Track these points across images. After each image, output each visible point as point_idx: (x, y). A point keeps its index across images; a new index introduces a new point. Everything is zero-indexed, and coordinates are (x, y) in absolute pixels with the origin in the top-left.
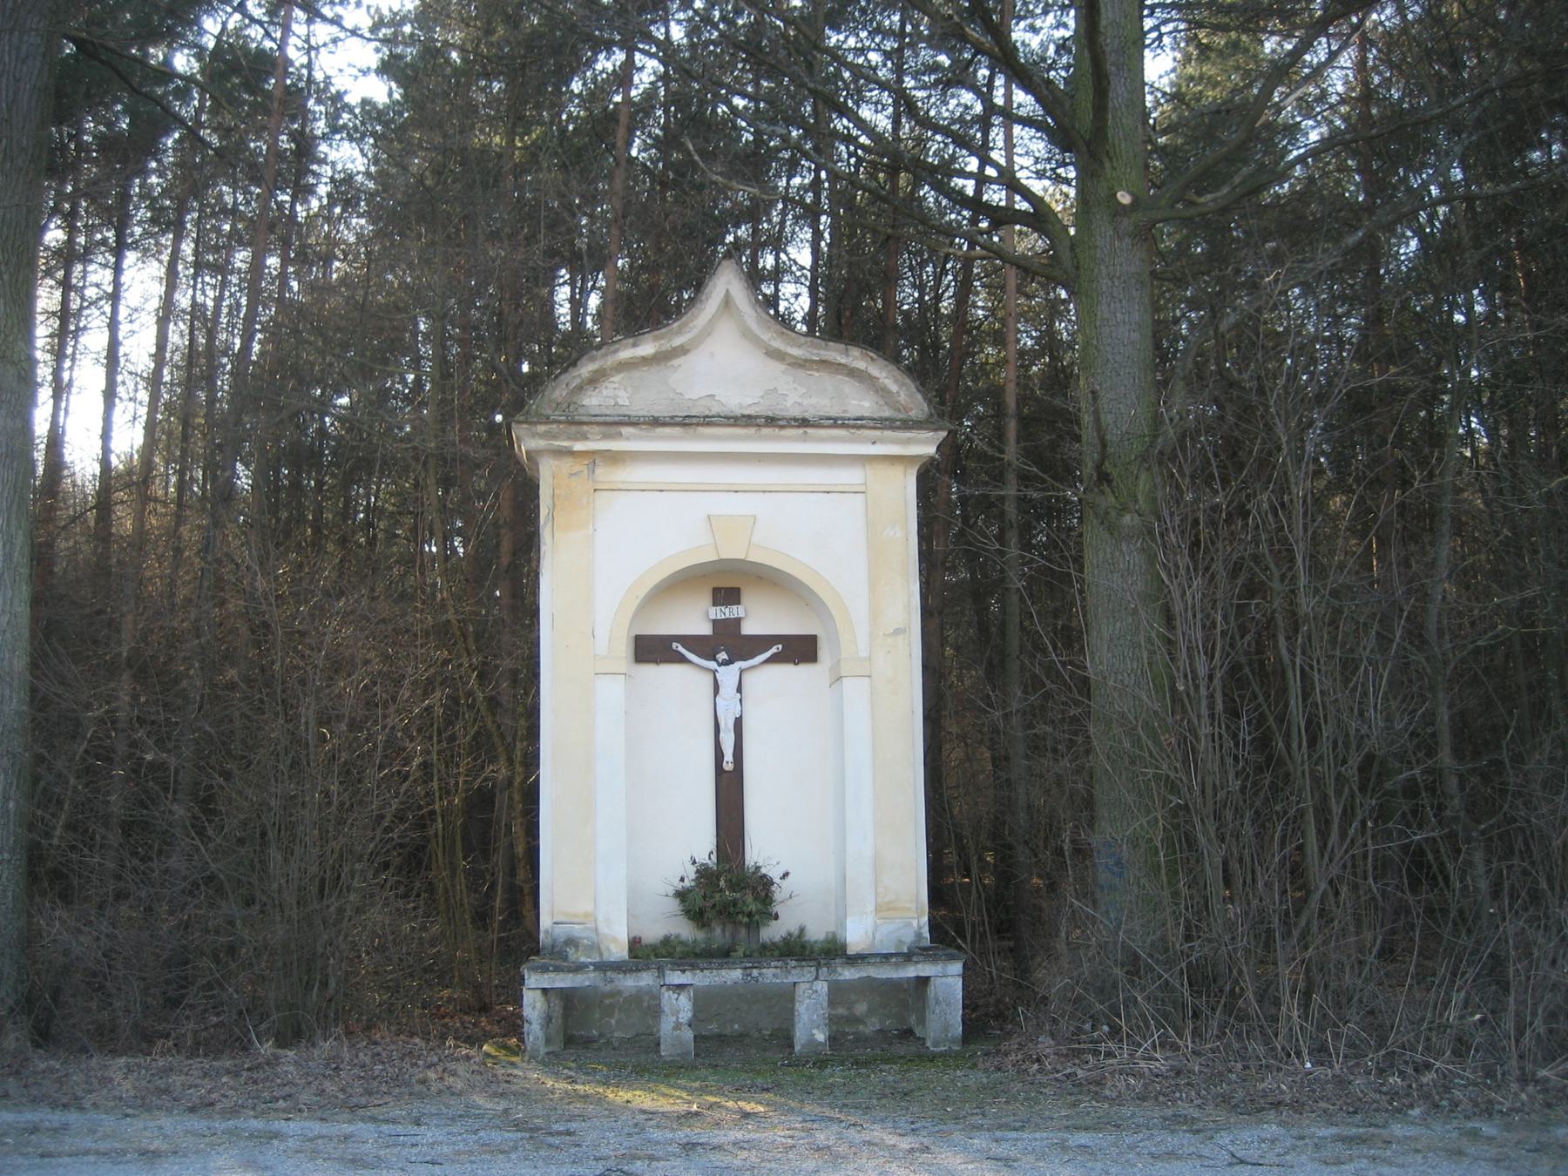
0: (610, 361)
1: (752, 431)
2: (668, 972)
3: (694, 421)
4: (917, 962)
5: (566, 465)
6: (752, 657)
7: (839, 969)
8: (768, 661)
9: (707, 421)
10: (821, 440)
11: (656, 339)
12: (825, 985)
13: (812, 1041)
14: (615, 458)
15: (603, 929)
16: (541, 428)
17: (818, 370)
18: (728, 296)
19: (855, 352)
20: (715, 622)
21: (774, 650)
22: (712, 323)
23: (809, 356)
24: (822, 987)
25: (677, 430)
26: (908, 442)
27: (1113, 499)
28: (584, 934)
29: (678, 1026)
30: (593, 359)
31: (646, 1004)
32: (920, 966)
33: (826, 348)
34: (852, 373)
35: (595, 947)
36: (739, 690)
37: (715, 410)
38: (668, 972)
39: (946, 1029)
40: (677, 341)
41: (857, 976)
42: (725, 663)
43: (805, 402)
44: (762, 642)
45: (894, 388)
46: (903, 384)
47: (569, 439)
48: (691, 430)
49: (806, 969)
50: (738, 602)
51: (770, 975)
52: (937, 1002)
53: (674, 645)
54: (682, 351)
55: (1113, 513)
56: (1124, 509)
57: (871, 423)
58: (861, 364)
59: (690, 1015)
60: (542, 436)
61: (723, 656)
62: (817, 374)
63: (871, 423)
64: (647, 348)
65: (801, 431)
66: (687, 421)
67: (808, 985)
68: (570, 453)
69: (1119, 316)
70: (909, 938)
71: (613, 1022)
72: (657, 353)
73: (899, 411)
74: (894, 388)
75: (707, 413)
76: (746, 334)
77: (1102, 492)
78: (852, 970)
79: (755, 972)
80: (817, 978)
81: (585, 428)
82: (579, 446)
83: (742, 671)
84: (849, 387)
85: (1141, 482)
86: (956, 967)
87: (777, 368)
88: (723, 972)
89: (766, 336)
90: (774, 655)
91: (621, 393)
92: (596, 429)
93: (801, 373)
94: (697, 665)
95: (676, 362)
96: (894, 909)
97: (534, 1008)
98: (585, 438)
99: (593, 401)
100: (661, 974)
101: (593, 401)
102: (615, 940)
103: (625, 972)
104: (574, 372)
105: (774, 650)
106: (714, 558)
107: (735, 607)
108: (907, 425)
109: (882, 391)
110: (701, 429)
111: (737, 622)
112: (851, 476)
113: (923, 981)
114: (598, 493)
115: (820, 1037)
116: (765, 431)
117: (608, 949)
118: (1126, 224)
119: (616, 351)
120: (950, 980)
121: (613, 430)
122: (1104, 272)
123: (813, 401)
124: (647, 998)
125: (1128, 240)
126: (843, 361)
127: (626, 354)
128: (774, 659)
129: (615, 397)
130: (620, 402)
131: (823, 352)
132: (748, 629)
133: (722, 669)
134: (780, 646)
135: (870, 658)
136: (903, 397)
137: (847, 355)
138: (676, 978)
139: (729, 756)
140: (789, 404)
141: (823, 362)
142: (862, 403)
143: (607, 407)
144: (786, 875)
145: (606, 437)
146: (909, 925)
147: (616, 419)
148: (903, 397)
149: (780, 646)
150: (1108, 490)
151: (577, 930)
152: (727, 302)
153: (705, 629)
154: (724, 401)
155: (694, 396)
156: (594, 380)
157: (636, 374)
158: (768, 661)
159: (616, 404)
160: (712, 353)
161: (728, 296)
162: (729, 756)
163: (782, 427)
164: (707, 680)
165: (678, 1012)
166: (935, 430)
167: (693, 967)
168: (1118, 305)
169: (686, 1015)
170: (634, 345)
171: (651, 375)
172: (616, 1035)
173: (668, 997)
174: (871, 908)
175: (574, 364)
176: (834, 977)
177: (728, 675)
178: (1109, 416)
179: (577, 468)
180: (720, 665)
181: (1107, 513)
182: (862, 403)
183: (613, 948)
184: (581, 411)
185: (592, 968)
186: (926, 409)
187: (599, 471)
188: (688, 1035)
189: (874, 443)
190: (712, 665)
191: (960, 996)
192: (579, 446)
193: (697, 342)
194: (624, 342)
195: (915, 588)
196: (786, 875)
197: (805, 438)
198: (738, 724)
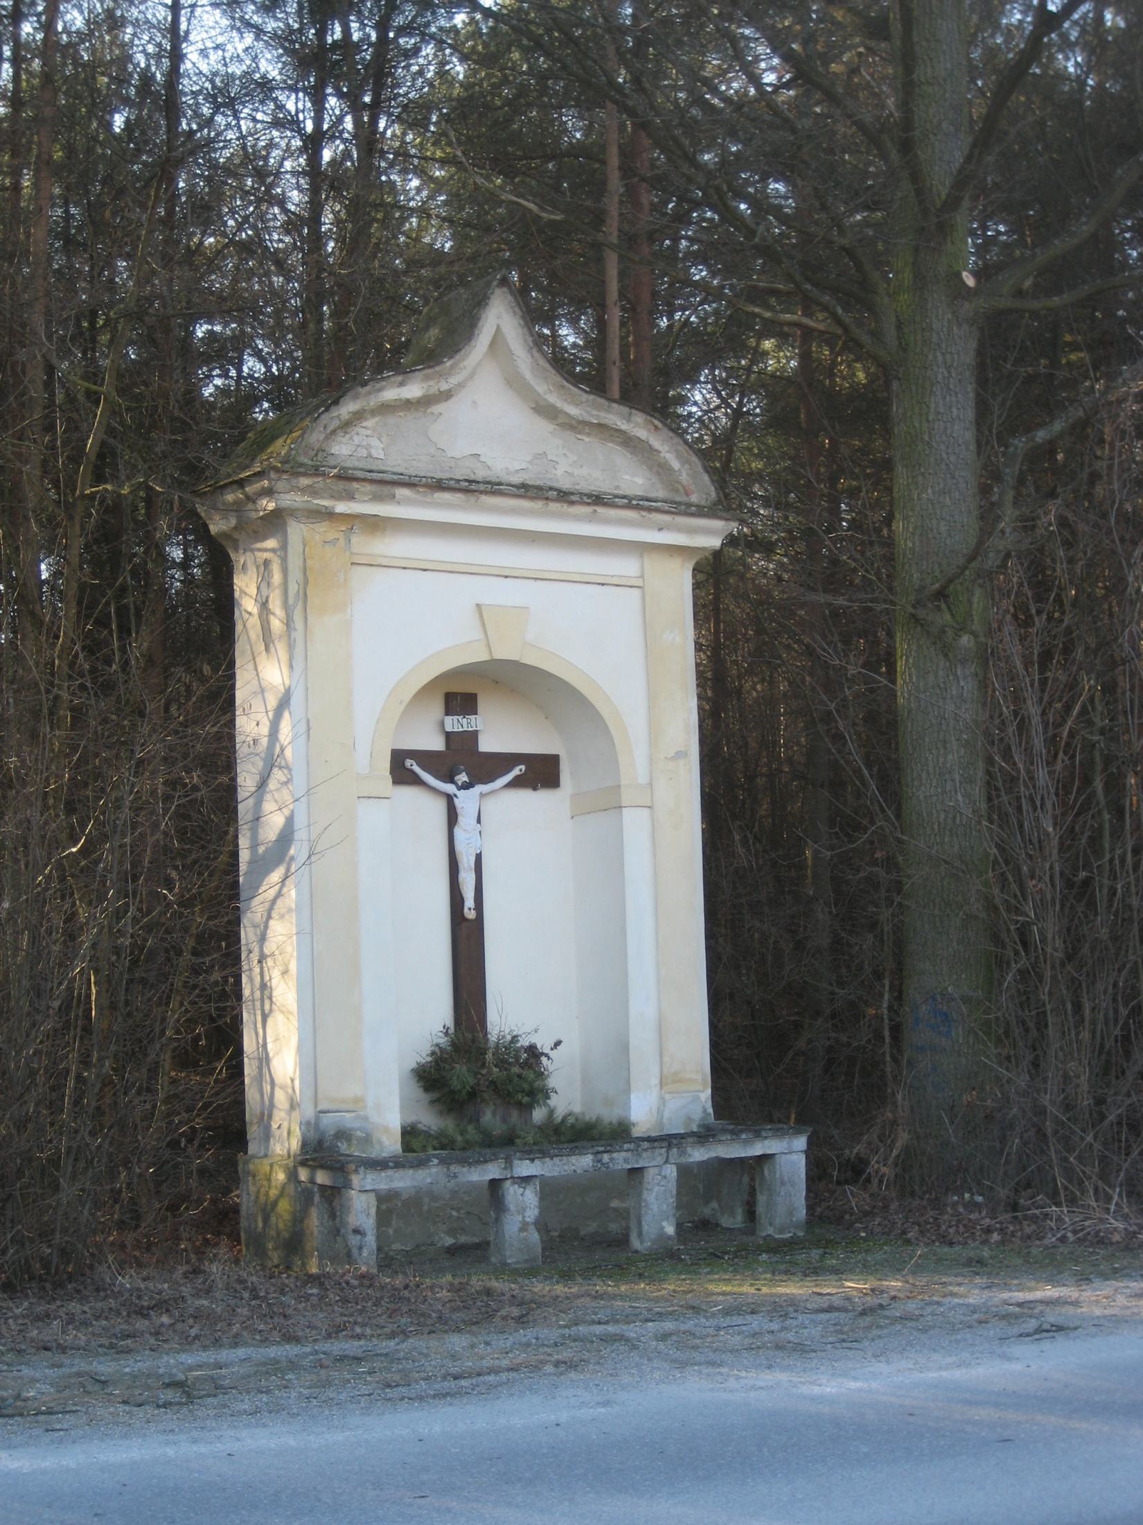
0: (373, 401)
1: (538, 505)
2: (516, 1162)
3: (482, 487)
4: (766, 1138)
5: (322, 530)
6: (493, 781)
7: (689, 1150)
8: (511, 785)
9: (494, 488)
10: (577, 518)
11: (427, 378)
12: (674, 1168)
13: (662, 1236)
14: (375, 525)
15: (375, 1118)
16: (304, 481)
17: (588, 434)
18: (498, 335)
19: (639, 418)
20: (448, 736)
21: (516, 772)
22: (479, 364)
23: (587, 418)
24: (671, 1171)
25: (459, 497)
26: (692, 531)
27: (947, 616)
28: (356, 1125)
29: (524, 1227)
30: (356, 397)
31: (426, 1208)
32: (766, 1142)
33: (608, 411)
34: (628, 441)
35: (367, 1140)
36: (479, 821)
37: (480, 474)
38: (516, 1162)
39: (791, 1213)
40: (444, 386)
41: (705, 1157)
42: (466, 786)
43: (576, 472)
44: (503, 762)
45: (676, 465)
46: (688, 462)
47: (332, 497)
48: (472, 498)
49: (657, 1151)
50: (474, 711)
51: (621, 1161)
52: (783, 1183)
53: (408, 763)
54: (446, 396)
55: (950, 633)
56: (961, 629)
57: (666, 507)
58: (642, 433)
59: (536, 1212)
60: (303, 490)
61: (463, 778)
62: (587, 439)
63: (666, 507)
64: (413, 390)
65: (589, 509)
66: (473, 487)
67: (656, 1170)
68: (330, 515)
69: (954, 410)
70: (697, 1115)
71: (391, 1231)
72: (424, 396)
73: (677, 491)
74: (676, 465)
75: (472, 477)
76: (514, 383)
77: (939, 608)
78: (702, 1150)
79: (606, 1157)
80: (667, 1162)
81: (355, 485)
82: (341, 507)
83: (482, 795)
84: (621, 458)
85: (975, 600)
86: (801, 1142)
87: (543, 427)
88: (573, 1159)
89: (541, 388)
90: (517, 777)
91: (375, 442)
92: (368, 487)
93: (570, 436)
94: (492, 792)
95: (436, 409)
96: (680, 1081)
97: (368, 1215)
98: (351, 497)
99: (343, 449)
100: (509, 1165)
101: (343, 449)
102: (386, 1129)
103: (470, 1164)
104: (335, 412)
105: (516, 772)
106: (485, 657)
107: (473, 717)
108: (700, 512)
109: (661, 469)
110: (484, 498)
111: (474, 736)
112: (626, 567)
113: (765, 1158)
114: (354, 567)
115: (670, 1230)
116: (554, 506)
117: (380, 1142)
118: (967, 308)
119: (380, 390)
120: (794, 1157)
121: (386, 490)
122: (940, 358)
123: (584, 471)
124: (426, 1200)
125: (965, 327)
126: (624, 427)
127: (391, 394)
128: (516, 783)
129: (368, 447)
130: (375, 454)
131: (603, 414)
132: (488, 744)
133: (461, 793)
134: (523, 767)
135: (651, 784)
136: (684, 477)
137: (629, 421)
138: (525, 1168)
139: (469, 902)
140: (560, 472)
141: (601, 426)
142: (635, 480)
143: (359, 459)
144: (558, 1044)
145: (377, 498)
146: (696, 1099)
147: (395, 477)
148: (684, 477)
149: (523, 767)
150: (944, 606)
151: (348, 1120)
152: (497, 341)
153: (436, 743)
154: (490, 462)
155: (458, 455)
156: (346, 426)
157: (392, 420)
158: (511, 785)
159: (370, 456)
160: (474, 402)
161: (498, 335)
162: (469, 902)
163: (572, 503)
164: (438, 808)
165: (524, 1209)
166: (727, 520)
167: (544, 1154)
168: (954, 399)
169: (532, 1213)
170: (401, 384)
171: (409, 422)
172: (394, 1247)
173: (512, 1193)
174: (655, 1081)
175: (336, 402)
176: (683, 1160)
177: (467, 801)
178: (943, 523)
179: (331, 535)
180: (460, 788)
181: (944, 632)
182: (635, 480)
183: (386, 1141)
184: (332, 462)
185: (391, 1164)
186: (713, 494)
187: (355, 539)
188: (534, 1237)
189: (660, 529)
190: (450, 788)
191: (803, 1176)
192: (341, 507)
193: (461, 386)
194: (393, 379)
195: (693, 703)
196: (558, 1044)
197: (592, 518)
198: (479, 858)
